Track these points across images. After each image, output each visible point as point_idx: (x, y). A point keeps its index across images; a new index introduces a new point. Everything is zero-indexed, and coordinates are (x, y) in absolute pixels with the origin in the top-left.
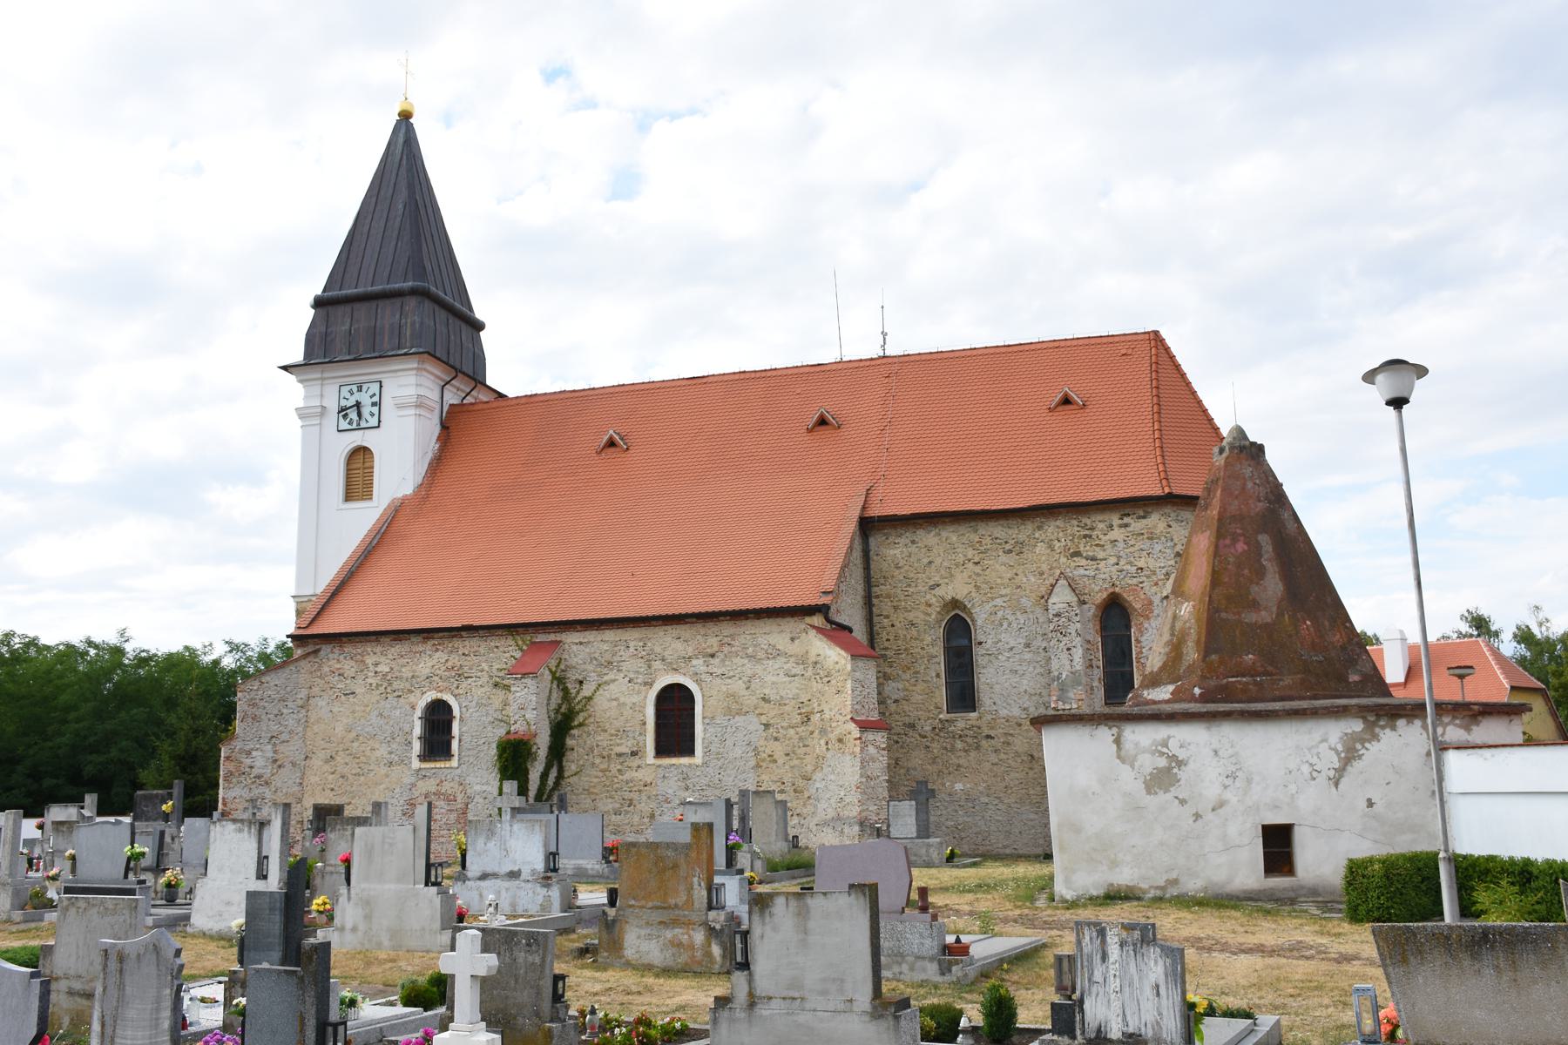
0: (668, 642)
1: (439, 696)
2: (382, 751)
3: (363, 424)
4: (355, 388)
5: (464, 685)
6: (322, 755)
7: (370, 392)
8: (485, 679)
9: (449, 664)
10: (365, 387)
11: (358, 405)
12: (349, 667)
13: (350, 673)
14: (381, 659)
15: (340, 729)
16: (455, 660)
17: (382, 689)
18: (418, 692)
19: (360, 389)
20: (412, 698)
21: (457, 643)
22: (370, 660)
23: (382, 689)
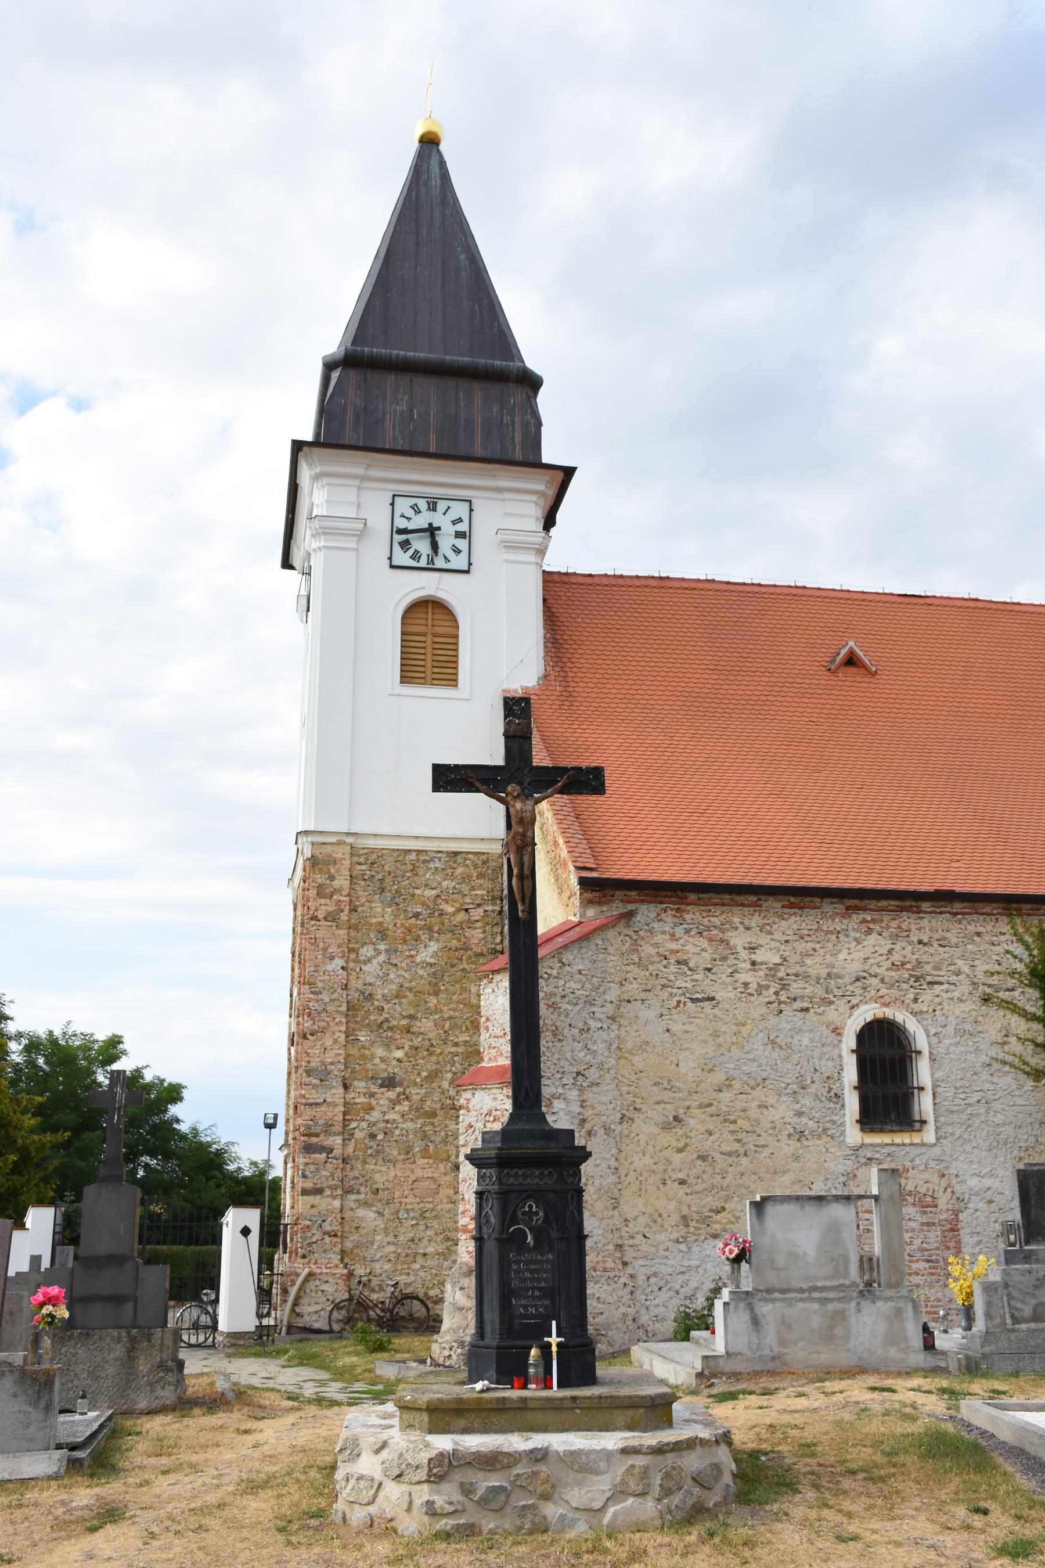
1: (889, 1013)
3: (440, 563)
4: (422, 504)
5: (927, 996)
7: (452, 515)
8: (965, 988)
9: (897, 958)
10: (442, 506)
11: (432, 531)
16: (904, 951)
17: (769, 994)
18: (842, 1005)
19: (432, 507)
20: (832, 1015)
21: (908, 921)
23: (769, 994)
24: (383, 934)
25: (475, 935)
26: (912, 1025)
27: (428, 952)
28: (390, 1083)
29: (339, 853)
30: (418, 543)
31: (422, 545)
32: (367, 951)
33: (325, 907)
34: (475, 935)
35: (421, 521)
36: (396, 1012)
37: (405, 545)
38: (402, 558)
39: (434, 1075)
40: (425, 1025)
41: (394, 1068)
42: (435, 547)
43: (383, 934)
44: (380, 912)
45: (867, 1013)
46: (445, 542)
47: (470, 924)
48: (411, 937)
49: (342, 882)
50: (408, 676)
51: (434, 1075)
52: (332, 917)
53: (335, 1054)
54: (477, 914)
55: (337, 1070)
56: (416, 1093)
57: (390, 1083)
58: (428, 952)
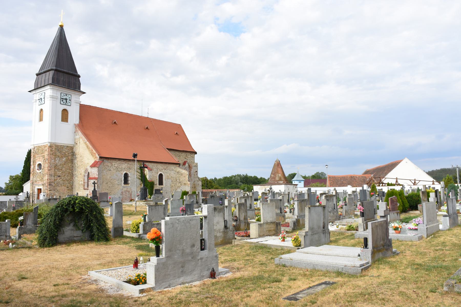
0: (160, 166)
2: (117, 182)
6: (105, 182)
12: (109, 165)
13: (110, 166)
14: (116, 164)
15: (108, 177)
22: (113, 164)
24: (59, 157)
25: (70, 157)
26: (129, 174)
27: (64, 159)
28: (59, 176)
29: (53, 145)
30: (64, 101)
31: (65, 101)
32: (57, 159)
33: (52, 153)
34: (70, 157)
35: (65, 97)
36: (60, 167)
37: (62, 101)
38: (62, 103)
39: (65, 176)
40: (64, 169)
41: (60, 175)
42: (66, 102)
43: (59, 157)
44: (58, 154)
45: (125, 172)
46: (68, 101)
47: (69, 156)
48: (62, 157)
49: (54, 149)
50: (62, 121)
51: (65, 176)
52: (52, 154)
53: (53, 173)
54: (70, 154)
55: (53, 175)
56: (62, 178)
57: (59, 176)
58: (64, 159)
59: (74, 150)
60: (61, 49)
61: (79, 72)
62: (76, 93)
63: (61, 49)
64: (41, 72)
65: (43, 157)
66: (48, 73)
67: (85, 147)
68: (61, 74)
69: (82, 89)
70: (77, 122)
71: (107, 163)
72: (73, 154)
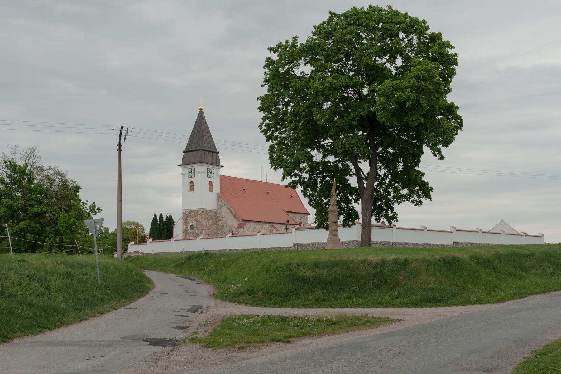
12: (249, 226)
58: (211, 221)
59: (217, 214)
60: (201, 128)
61: (218, 150)
62: (218, 167)
63: (201, 128)
64: (187, 150)
65: (196, 219)
66: (196, 152)
67: (228, 211)
68: (207, 153)
69: (221, 164)
70: (219, 191)
71: (247, 224)
72: (217, 217)
